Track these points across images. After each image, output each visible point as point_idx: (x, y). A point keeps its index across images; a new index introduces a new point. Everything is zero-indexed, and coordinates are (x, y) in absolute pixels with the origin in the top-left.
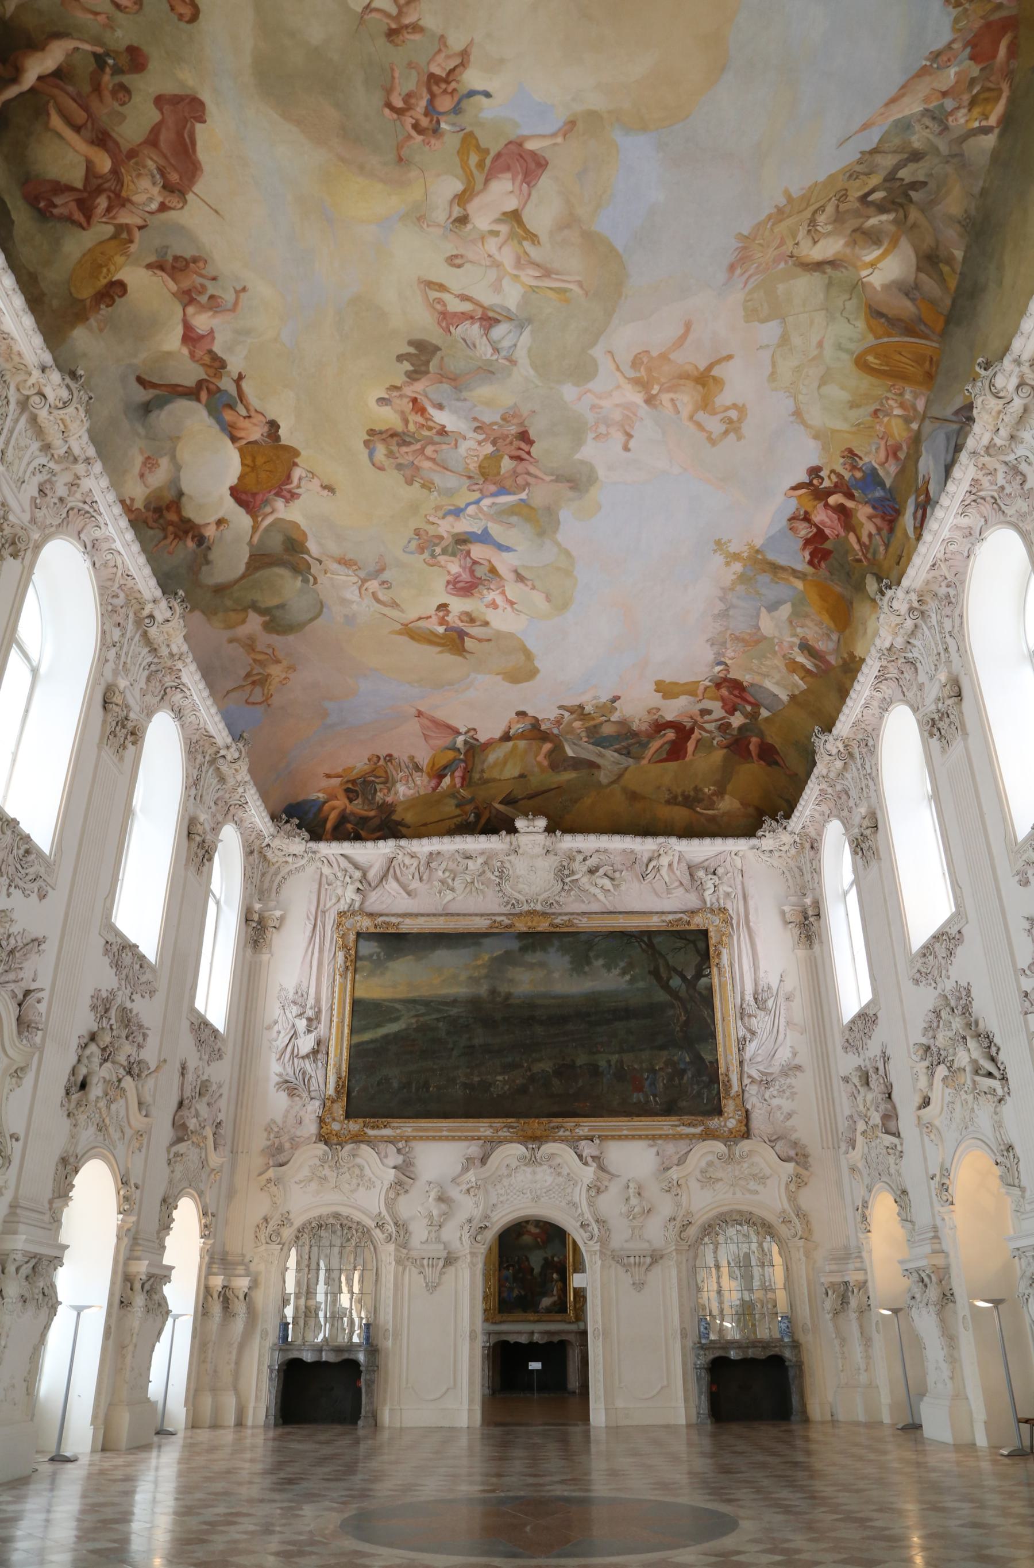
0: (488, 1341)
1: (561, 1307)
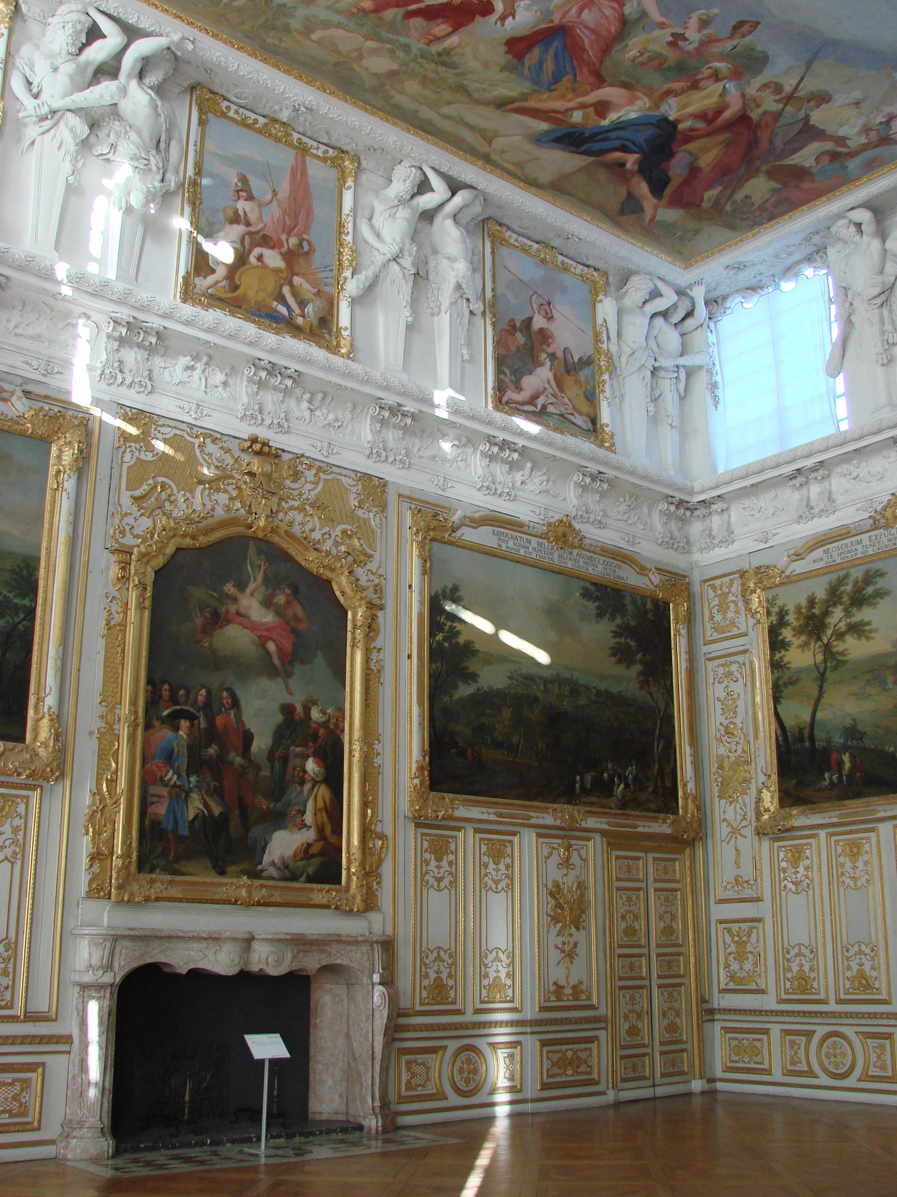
0: (108, 967)
1: (323, 865)
